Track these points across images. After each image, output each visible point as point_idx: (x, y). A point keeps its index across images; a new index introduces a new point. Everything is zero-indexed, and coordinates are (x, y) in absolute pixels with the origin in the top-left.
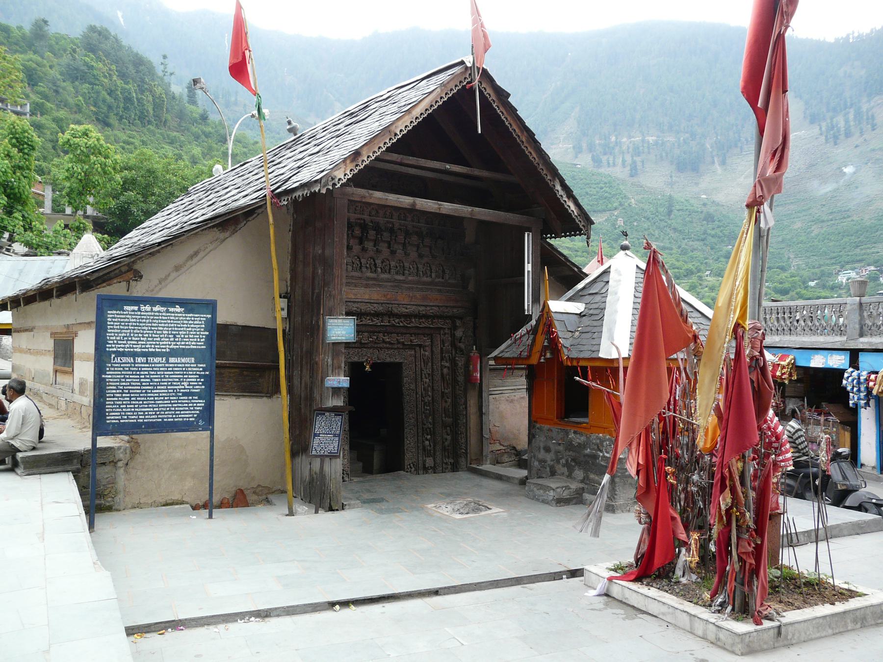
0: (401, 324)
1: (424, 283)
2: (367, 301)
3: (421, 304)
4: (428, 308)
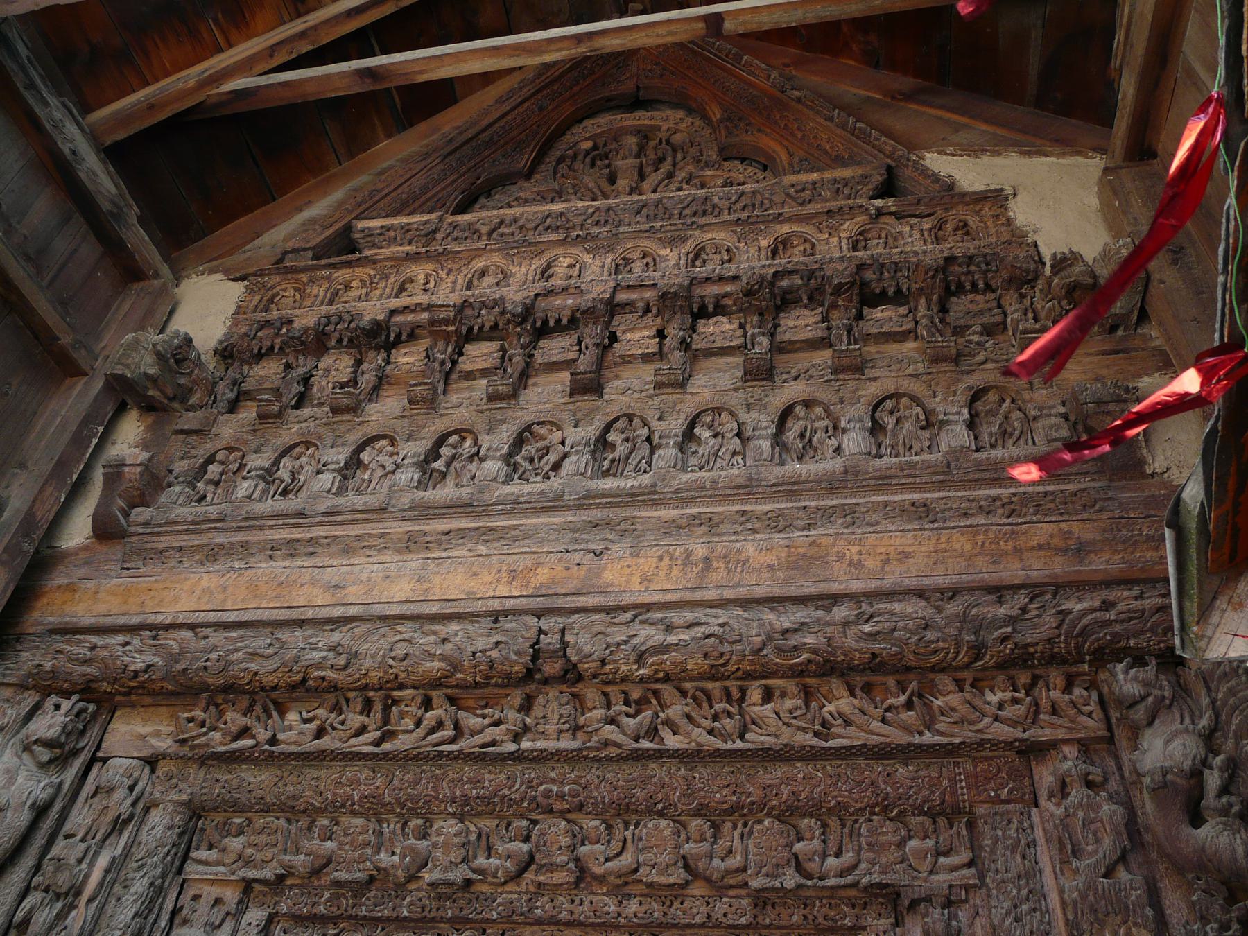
0: (672, 742)
1: (791, 489)
2: (394, 610)
3: (793, 591)
4: (842, 612)
